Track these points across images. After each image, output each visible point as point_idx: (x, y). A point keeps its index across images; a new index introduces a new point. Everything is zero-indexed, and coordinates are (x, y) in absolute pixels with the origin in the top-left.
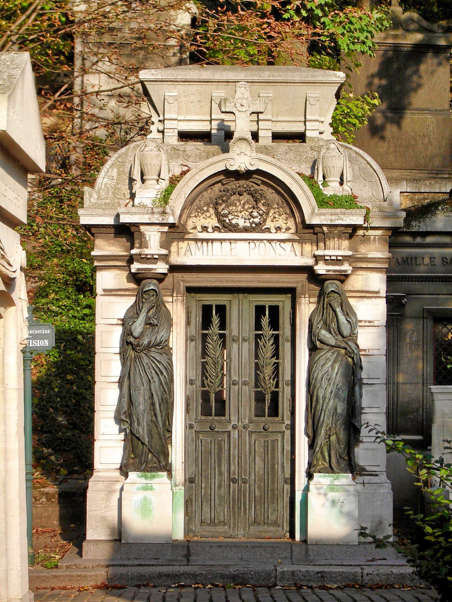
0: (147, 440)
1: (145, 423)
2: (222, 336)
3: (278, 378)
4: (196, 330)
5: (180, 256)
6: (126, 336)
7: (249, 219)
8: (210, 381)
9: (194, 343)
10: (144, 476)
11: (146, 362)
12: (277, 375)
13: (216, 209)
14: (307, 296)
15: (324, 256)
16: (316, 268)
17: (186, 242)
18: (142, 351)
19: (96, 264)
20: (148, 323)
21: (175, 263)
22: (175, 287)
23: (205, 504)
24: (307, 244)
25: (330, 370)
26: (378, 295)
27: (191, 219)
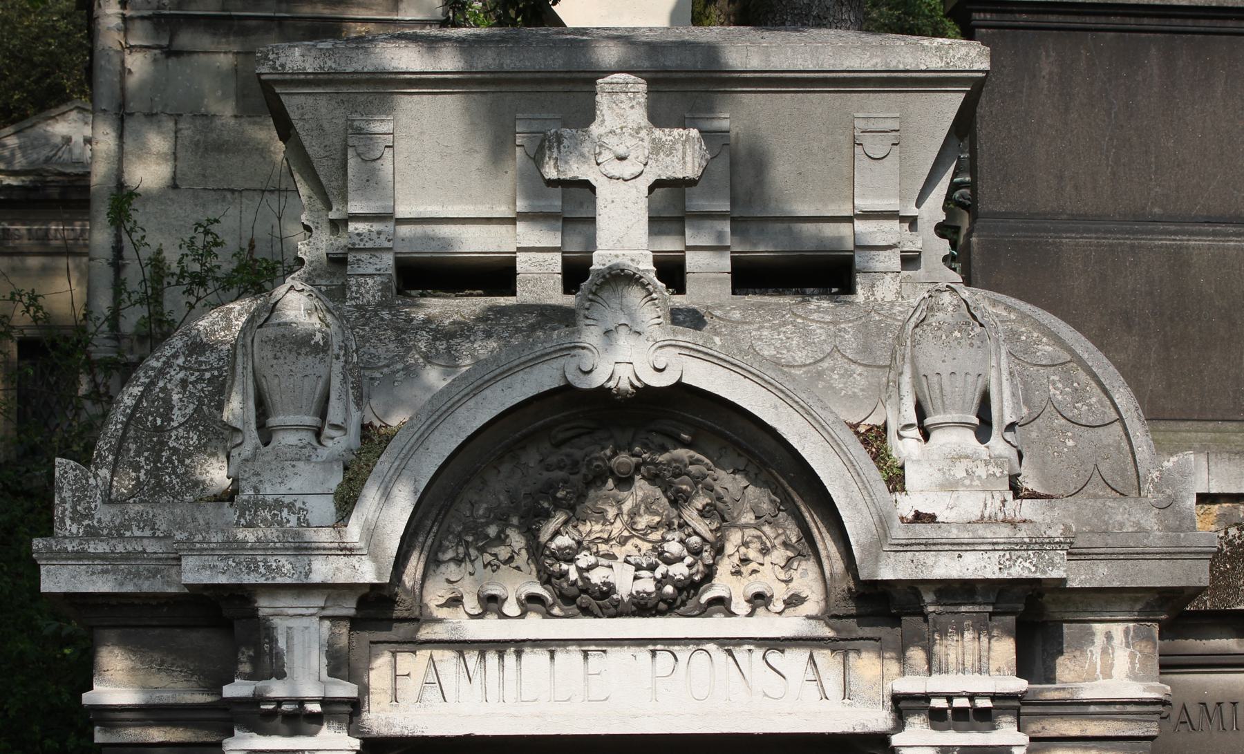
5: (402, 704)
7: (652, 568)
13: (531, 534)
15: (927, 697)
16: (896, 740)
17: (424, 654)
21: (385, 731)
24: (864, 655)
27: (443, 568)
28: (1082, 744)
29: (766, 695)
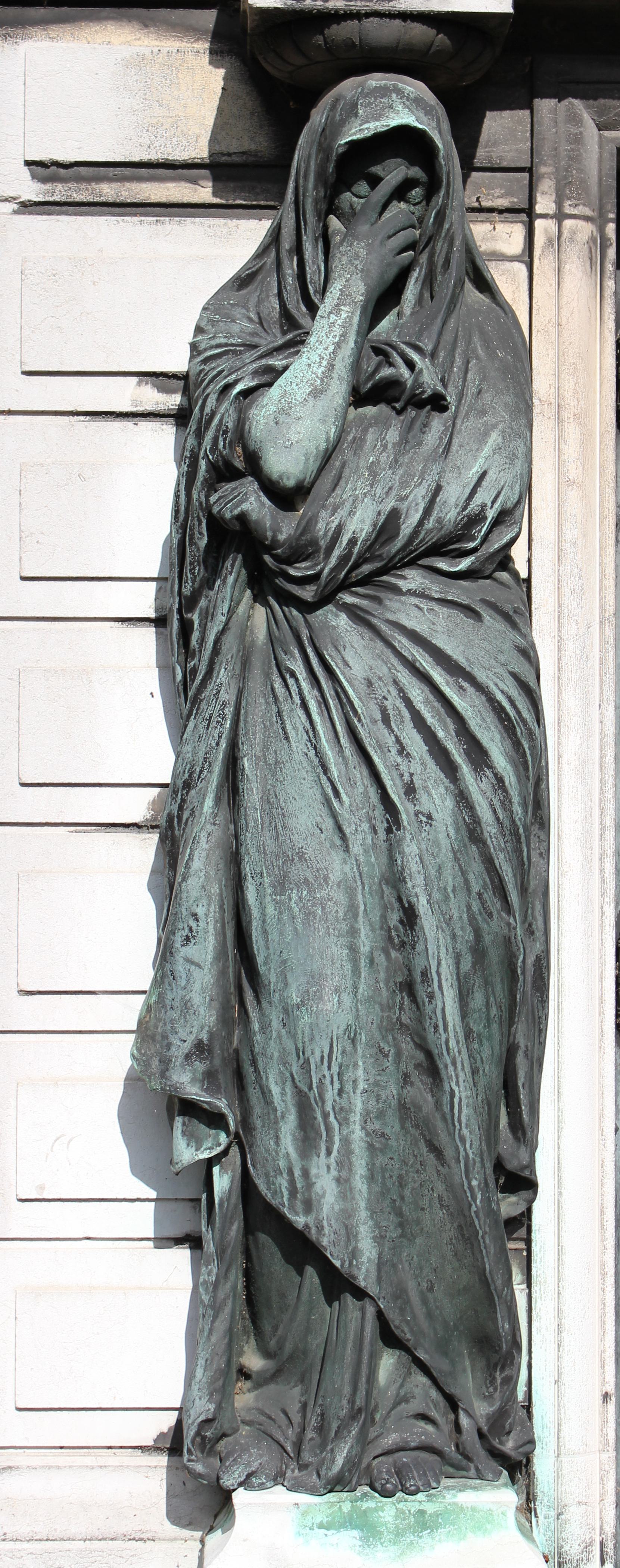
0: (368, 1250)
1: (357, 1135)
6: (211, 486)
18: (325, 599)
22: (546, 150)
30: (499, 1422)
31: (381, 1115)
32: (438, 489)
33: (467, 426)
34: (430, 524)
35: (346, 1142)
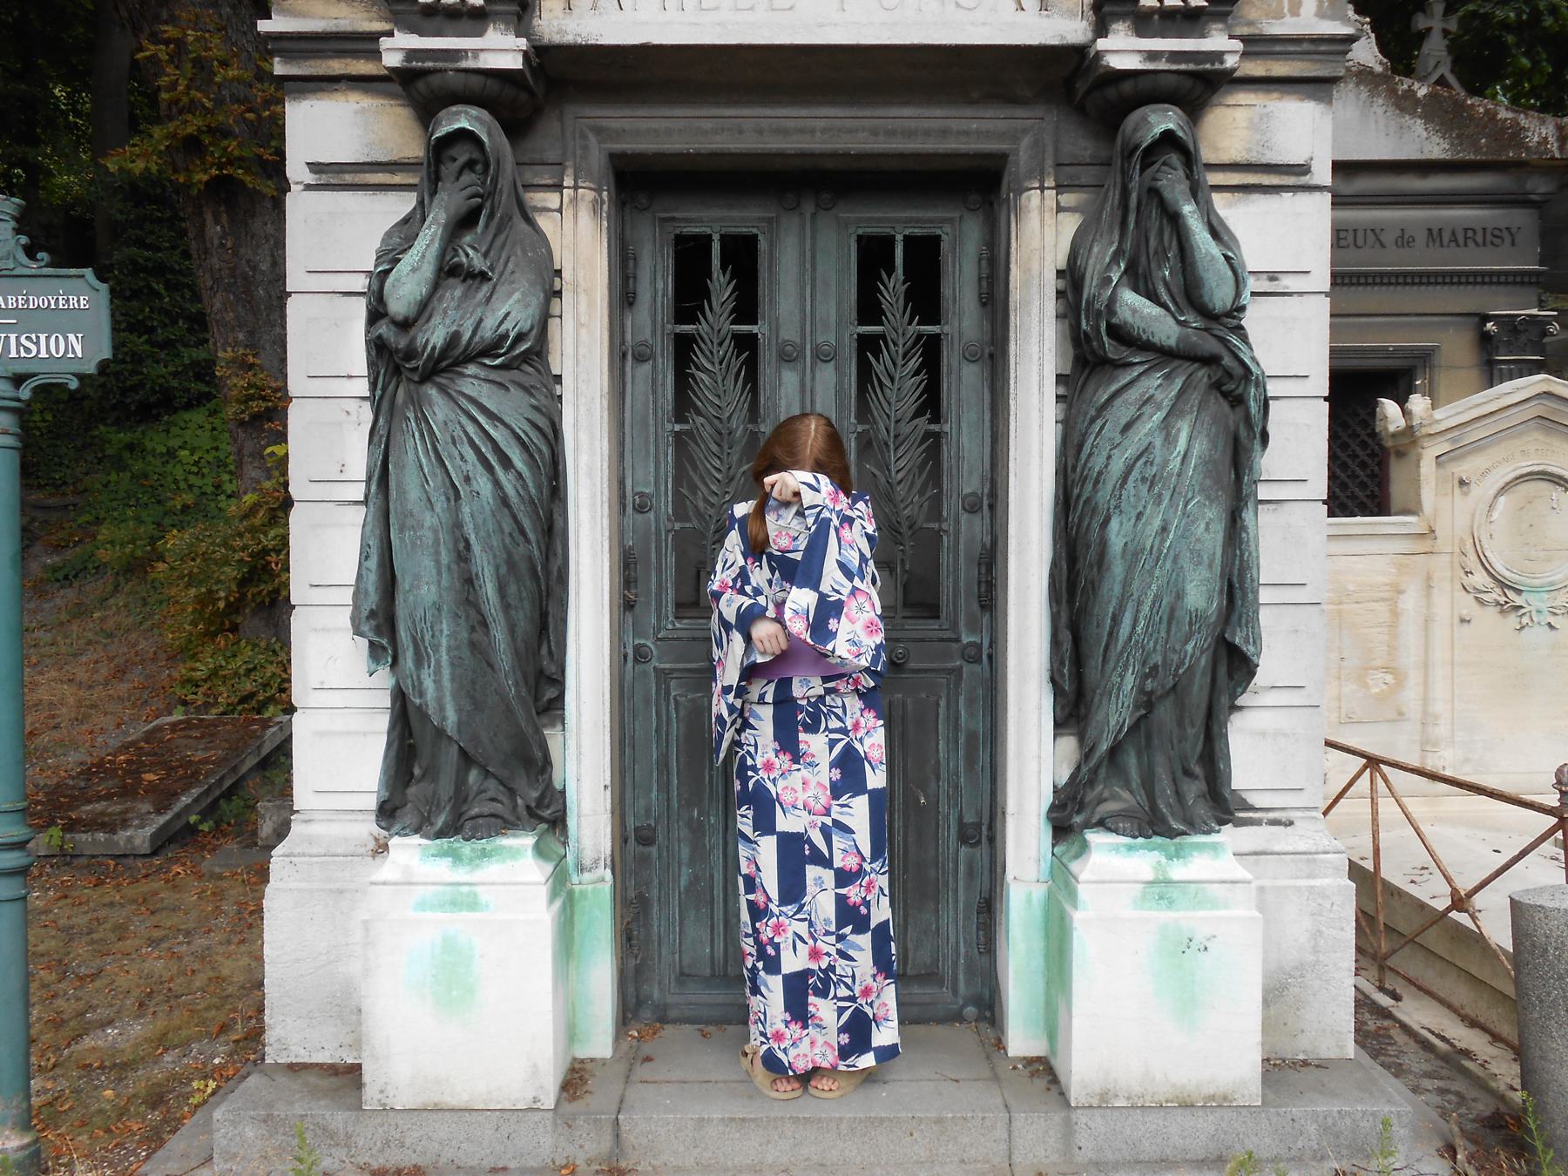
0: (451, 717)
1: (445, 658)
2: (747, 345)
3: (938, 485)
4: (654, 322)
5: (576, 11)
8: (706, 500)
9: (646, 368)
10: (442, 854)
11: (440, 416)
12: (935, 477)
14: (1050, 182)
19: (279, 68)
20: (448, 271)
21: (557, 39)
23: (692, 913)
25: (1158, 442)
26: (1304, 180)
28: (1265, 87)
29: (958, 5)
30: (540, 802)
31: (458, 648)
32: (481, 320)
33: (501, 290)
34: (477, 339)
35: (438, 663)
